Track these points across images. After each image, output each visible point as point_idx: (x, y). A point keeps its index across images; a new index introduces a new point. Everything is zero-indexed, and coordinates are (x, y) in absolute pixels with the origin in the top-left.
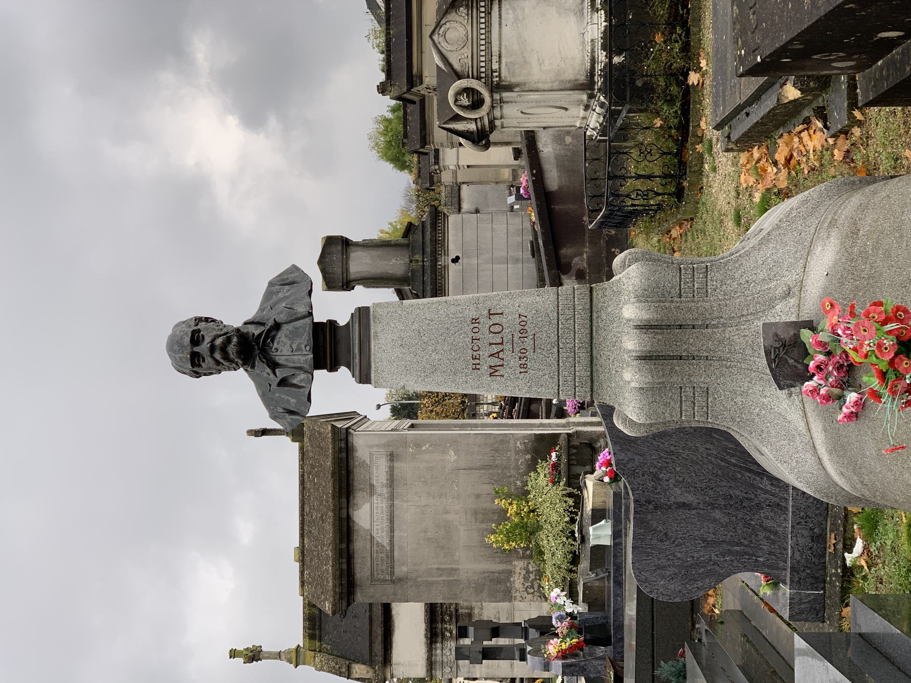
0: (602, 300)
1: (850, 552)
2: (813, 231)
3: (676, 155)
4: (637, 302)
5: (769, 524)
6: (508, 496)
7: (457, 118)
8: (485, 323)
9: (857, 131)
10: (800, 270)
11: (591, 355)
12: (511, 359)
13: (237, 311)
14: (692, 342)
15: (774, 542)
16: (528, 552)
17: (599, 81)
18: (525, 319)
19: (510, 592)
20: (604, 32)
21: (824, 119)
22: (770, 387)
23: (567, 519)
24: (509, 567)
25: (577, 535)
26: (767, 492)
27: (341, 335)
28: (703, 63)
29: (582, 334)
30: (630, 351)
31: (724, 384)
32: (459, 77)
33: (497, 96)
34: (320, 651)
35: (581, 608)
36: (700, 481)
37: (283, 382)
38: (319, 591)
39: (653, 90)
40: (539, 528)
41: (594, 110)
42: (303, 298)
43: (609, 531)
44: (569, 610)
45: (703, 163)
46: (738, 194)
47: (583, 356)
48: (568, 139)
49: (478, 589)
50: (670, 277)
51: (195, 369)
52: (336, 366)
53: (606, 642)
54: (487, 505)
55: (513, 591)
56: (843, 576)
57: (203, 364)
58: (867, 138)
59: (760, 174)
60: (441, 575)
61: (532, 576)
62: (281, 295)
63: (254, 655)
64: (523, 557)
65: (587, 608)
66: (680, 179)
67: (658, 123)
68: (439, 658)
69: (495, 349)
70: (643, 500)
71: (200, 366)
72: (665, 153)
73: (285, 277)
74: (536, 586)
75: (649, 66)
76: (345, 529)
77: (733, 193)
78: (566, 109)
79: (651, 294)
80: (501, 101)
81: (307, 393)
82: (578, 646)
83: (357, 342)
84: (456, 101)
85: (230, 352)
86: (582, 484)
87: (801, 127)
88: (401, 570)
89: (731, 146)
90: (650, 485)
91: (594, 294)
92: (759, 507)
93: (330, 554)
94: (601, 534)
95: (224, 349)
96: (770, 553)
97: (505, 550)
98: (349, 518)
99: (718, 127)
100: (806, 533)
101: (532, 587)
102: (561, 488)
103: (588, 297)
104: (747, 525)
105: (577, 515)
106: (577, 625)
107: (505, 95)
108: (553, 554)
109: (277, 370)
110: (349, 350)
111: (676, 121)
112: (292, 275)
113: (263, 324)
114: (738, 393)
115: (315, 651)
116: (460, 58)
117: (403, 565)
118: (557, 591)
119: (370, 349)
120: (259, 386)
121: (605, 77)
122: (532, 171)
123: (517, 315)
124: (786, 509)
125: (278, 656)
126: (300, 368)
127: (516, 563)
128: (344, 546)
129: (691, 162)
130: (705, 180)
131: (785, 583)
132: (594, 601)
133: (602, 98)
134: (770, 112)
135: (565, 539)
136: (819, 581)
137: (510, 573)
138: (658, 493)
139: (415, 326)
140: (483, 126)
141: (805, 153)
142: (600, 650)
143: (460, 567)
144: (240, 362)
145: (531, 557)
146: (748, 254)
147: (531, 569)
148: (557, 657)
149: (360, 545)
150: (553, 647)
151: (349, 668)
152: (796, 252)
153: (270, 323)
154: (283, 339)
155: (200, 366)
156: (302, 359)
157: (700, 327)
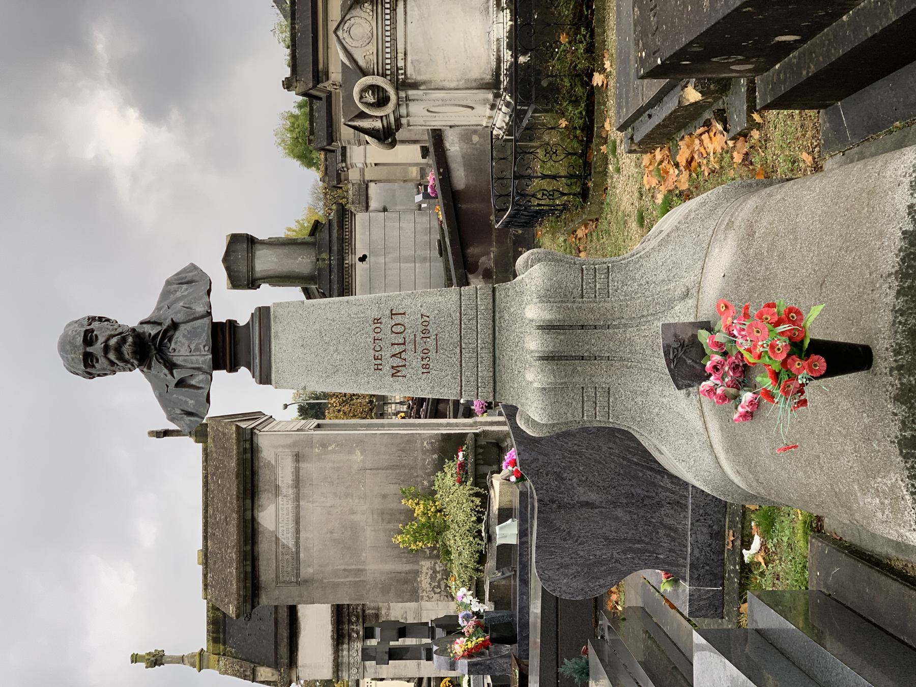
0: (505, 300)
2: (711, 233)
3: (581, 156)
4: (540, 302)
5: (669, 521)
6: (415, 496)
7: (362, 115)
8: (387, 323)
9: (756, 134)
10: (698, 271)
11: (494, 356)
12: (414, 360)
13: (133, 310)
14: (594, 343)
15: (674, 540)
16: (435, 552)
17: (505, 81)
18: (428, 319)
19: (417, 592)
20: (510, 32)
21: (725, 122)
23: (474, 518)
24: (416, 567)
25: (483, 534)
26: (667, 490)
27: (241, 335)
28: (607, 65)
29: (485, 335)
30: (532, 352)
31: (625, 384)
32: (364, 73)
33: (402, 94)
34: (224, 655)
35: (487, 607)
36: (603, 480)
37: (181, 383)
38: (223, 594)
39: (558, 91)
40: (446, 528)
41: (500, 110)
42: (201, 298)
43: (515, 531)
44: (475, 609)
45: (607, 164)
46: (641, 195)
47: (486, 356)
48: (475, 139)
49: (385, 589)
50: (572, 278)
51: (89, 370)
52: (235, 366)
53: (511, 640)
54: (394, 505)
55: (420, 591)
56: (741, 573)
57: (96, 365)
58: (766, 141)
59: (663, 176)
60: (347, 576)
61: (439, 576)
62: (179, 294)
63: (156, 660)
64: (431, 557)
65: (493, 606)
66: (585, 180)
67: (563, 123)
68: (345, 660)
69: (397, 349)
70: (546, 499)
71: (93, 366)
72: (569, 154)
73: (184, 275)
74: (443, 586)
75: (554, 66)
76: (249, 531)
77: (637, 194)
78: (473, 108)
79: (554, 295)
80: (407, 99)
81: (206, 394)
82: (484, 645)
83: (257, 342)
84: (361, 98)
85: (125, 353)
86: (489, 484)
87: (702, 129)
88: (307, 571)
89: (634, 147)
90: (554, 484)
91: (497, 293)
92: (659, 505)
93: (234, 557)
94: (507, 533)
95: (118, 350)
96: (670, 550)
97: (412, 550)
98: (253, 519)
99: (622, 128)
100: (705, 530)
101: (439, 586)
102: (468, 488)
103: (490, 297)
104: (648, 522)
105: (484, 514)
106: (483, 623)
107: (412, 93)
108: (460, 554)
109: (174, 371)
110: (249, 351)
111: (581, 121)
112: (191, 274)
113: (160, 324)
115: (219, 654)
116: (365, 55)
117: (309, 566)
118: (464, 590)
119: (270, 349)
120: (155, 388)
121: (510, 76)
122: (438, 170)
123: (419, 316)
124: (686, 506)
125: (181, 660)
126: (199, 369)
127: (423, 563)
128: (249, 548)
129: (596, 163)
130: (609, 181)
131: (685, 580)
132: (501, 599)
133: (508, 98)
134: (671, 114)
135: (471, 539)
136: (718, 577)
137: (417, 573)
138: (561, 493)
139: (317, 326)
140: (389, 124)
141: (705, 155)
142: (506, 649)
143: (367, 568)
144: (136, 362)
145: (438, 557)
146: (648, 255)
147: (438, 569)
148: (463, 656)
149: (265, 547)
150: (460, 646)
151: (254, 672)
152: (694, 254)
153: (168, 323)
154: (181, 339)
155: (93, 366)
156: (201, 359)
157: (602, 327)
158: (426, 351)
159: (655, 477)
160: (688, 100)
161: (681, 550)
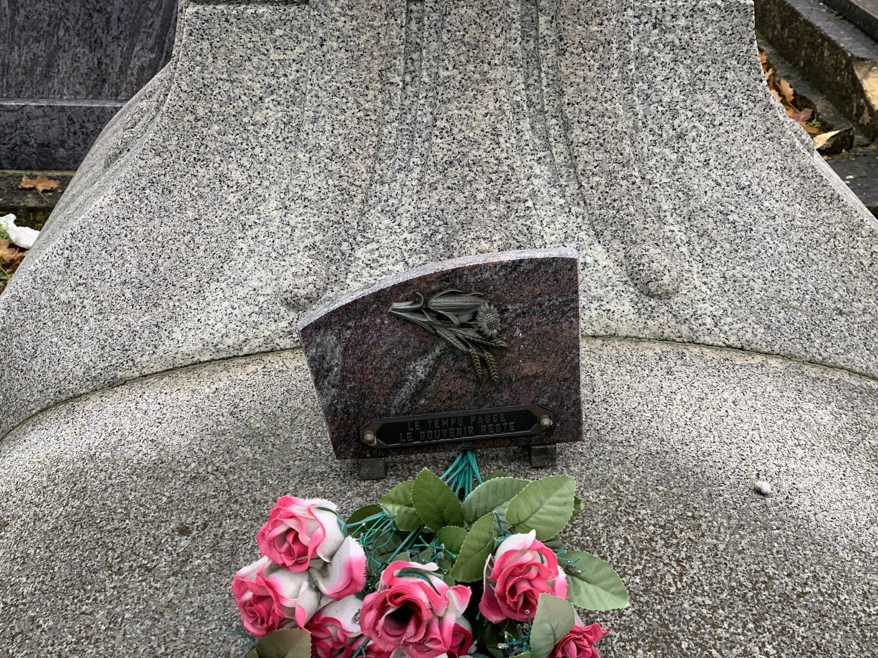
1: (18, 223)
5: (64, 64)
22: (320, 227)
26: (127, 58)
31: (322, 61)
87: (788, 91)
92: (95, 44)
100: (54, 133)
104: (56, 21)
114: (295, 111)
124: (98, 96)
152: (786, 306)
159: (149, 35)
160: (866, 76)
161: (9, 86)
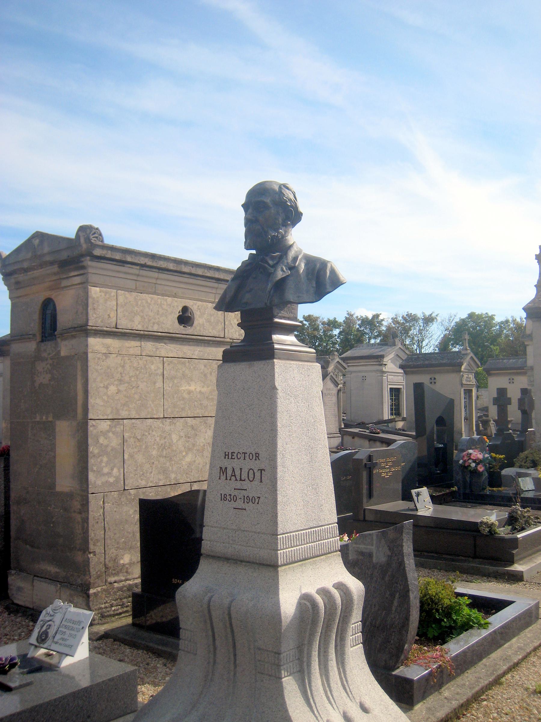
69: (237, 473)
158: (235, 499)
